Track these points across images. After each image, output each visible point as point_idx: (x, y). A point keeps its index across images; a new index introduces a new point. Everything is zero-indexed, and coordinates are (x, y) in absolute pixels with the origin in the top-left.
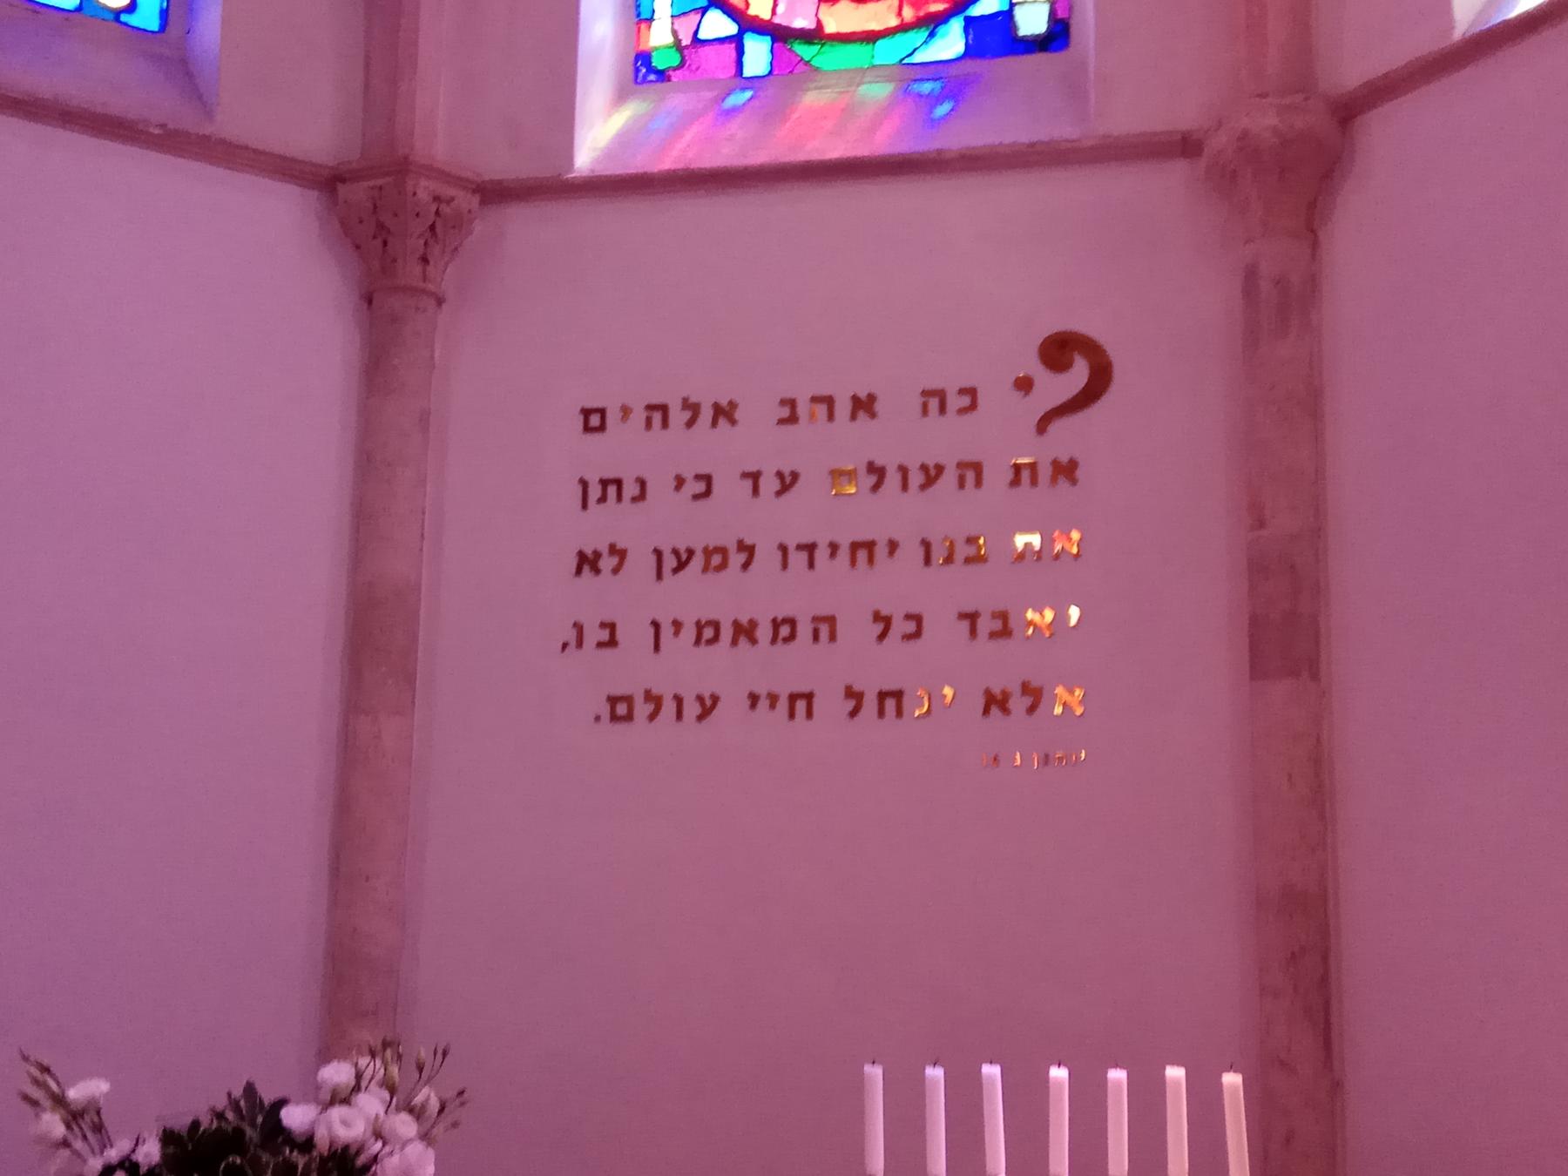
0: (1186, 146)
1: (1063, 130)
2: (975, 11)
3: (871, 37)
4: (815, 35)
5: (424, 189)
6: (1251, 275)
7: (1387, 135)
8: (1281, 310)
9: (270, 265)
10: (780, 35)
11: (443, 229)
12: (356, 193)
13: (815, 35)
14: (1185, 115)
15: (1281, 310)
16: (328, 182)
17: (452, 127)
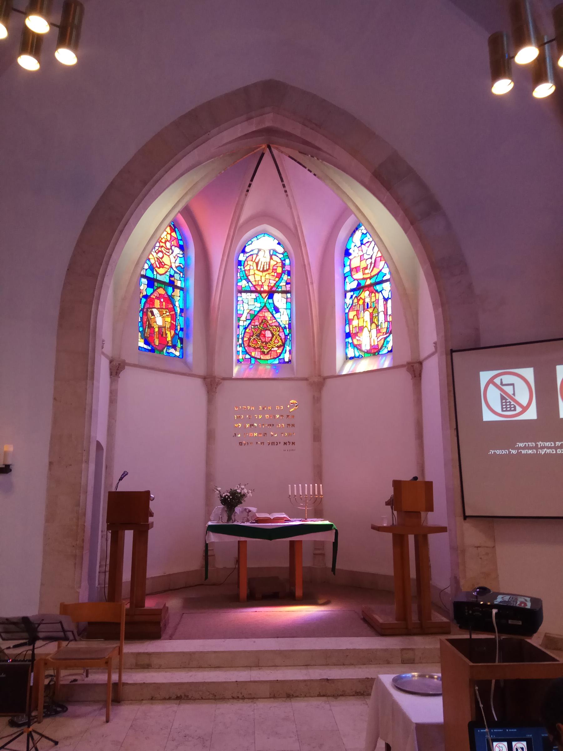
0: (306, 379)
1: (293, 376)
2: (280, 358)
3: (267, 360)
4: (260, 359)
5: (217, 380)
6: (314, 397)
7: (329, 381)
8: (317, 400)
9: (195, 388)
10: (256, 358)
11: (218, 384)
12: (209, 380)
13: (260, 359)
14: (306, 376)
15: (317, 400)
16: (204, 378)
17: (218, 371)
